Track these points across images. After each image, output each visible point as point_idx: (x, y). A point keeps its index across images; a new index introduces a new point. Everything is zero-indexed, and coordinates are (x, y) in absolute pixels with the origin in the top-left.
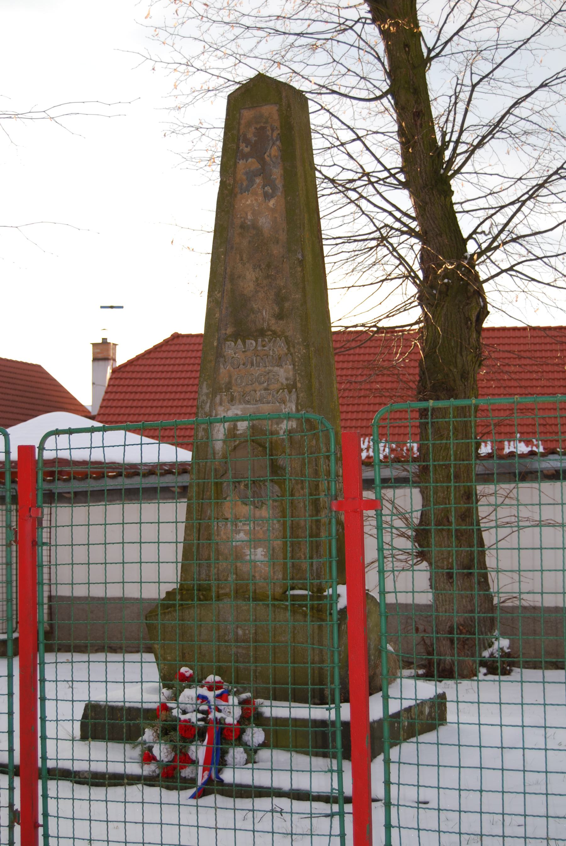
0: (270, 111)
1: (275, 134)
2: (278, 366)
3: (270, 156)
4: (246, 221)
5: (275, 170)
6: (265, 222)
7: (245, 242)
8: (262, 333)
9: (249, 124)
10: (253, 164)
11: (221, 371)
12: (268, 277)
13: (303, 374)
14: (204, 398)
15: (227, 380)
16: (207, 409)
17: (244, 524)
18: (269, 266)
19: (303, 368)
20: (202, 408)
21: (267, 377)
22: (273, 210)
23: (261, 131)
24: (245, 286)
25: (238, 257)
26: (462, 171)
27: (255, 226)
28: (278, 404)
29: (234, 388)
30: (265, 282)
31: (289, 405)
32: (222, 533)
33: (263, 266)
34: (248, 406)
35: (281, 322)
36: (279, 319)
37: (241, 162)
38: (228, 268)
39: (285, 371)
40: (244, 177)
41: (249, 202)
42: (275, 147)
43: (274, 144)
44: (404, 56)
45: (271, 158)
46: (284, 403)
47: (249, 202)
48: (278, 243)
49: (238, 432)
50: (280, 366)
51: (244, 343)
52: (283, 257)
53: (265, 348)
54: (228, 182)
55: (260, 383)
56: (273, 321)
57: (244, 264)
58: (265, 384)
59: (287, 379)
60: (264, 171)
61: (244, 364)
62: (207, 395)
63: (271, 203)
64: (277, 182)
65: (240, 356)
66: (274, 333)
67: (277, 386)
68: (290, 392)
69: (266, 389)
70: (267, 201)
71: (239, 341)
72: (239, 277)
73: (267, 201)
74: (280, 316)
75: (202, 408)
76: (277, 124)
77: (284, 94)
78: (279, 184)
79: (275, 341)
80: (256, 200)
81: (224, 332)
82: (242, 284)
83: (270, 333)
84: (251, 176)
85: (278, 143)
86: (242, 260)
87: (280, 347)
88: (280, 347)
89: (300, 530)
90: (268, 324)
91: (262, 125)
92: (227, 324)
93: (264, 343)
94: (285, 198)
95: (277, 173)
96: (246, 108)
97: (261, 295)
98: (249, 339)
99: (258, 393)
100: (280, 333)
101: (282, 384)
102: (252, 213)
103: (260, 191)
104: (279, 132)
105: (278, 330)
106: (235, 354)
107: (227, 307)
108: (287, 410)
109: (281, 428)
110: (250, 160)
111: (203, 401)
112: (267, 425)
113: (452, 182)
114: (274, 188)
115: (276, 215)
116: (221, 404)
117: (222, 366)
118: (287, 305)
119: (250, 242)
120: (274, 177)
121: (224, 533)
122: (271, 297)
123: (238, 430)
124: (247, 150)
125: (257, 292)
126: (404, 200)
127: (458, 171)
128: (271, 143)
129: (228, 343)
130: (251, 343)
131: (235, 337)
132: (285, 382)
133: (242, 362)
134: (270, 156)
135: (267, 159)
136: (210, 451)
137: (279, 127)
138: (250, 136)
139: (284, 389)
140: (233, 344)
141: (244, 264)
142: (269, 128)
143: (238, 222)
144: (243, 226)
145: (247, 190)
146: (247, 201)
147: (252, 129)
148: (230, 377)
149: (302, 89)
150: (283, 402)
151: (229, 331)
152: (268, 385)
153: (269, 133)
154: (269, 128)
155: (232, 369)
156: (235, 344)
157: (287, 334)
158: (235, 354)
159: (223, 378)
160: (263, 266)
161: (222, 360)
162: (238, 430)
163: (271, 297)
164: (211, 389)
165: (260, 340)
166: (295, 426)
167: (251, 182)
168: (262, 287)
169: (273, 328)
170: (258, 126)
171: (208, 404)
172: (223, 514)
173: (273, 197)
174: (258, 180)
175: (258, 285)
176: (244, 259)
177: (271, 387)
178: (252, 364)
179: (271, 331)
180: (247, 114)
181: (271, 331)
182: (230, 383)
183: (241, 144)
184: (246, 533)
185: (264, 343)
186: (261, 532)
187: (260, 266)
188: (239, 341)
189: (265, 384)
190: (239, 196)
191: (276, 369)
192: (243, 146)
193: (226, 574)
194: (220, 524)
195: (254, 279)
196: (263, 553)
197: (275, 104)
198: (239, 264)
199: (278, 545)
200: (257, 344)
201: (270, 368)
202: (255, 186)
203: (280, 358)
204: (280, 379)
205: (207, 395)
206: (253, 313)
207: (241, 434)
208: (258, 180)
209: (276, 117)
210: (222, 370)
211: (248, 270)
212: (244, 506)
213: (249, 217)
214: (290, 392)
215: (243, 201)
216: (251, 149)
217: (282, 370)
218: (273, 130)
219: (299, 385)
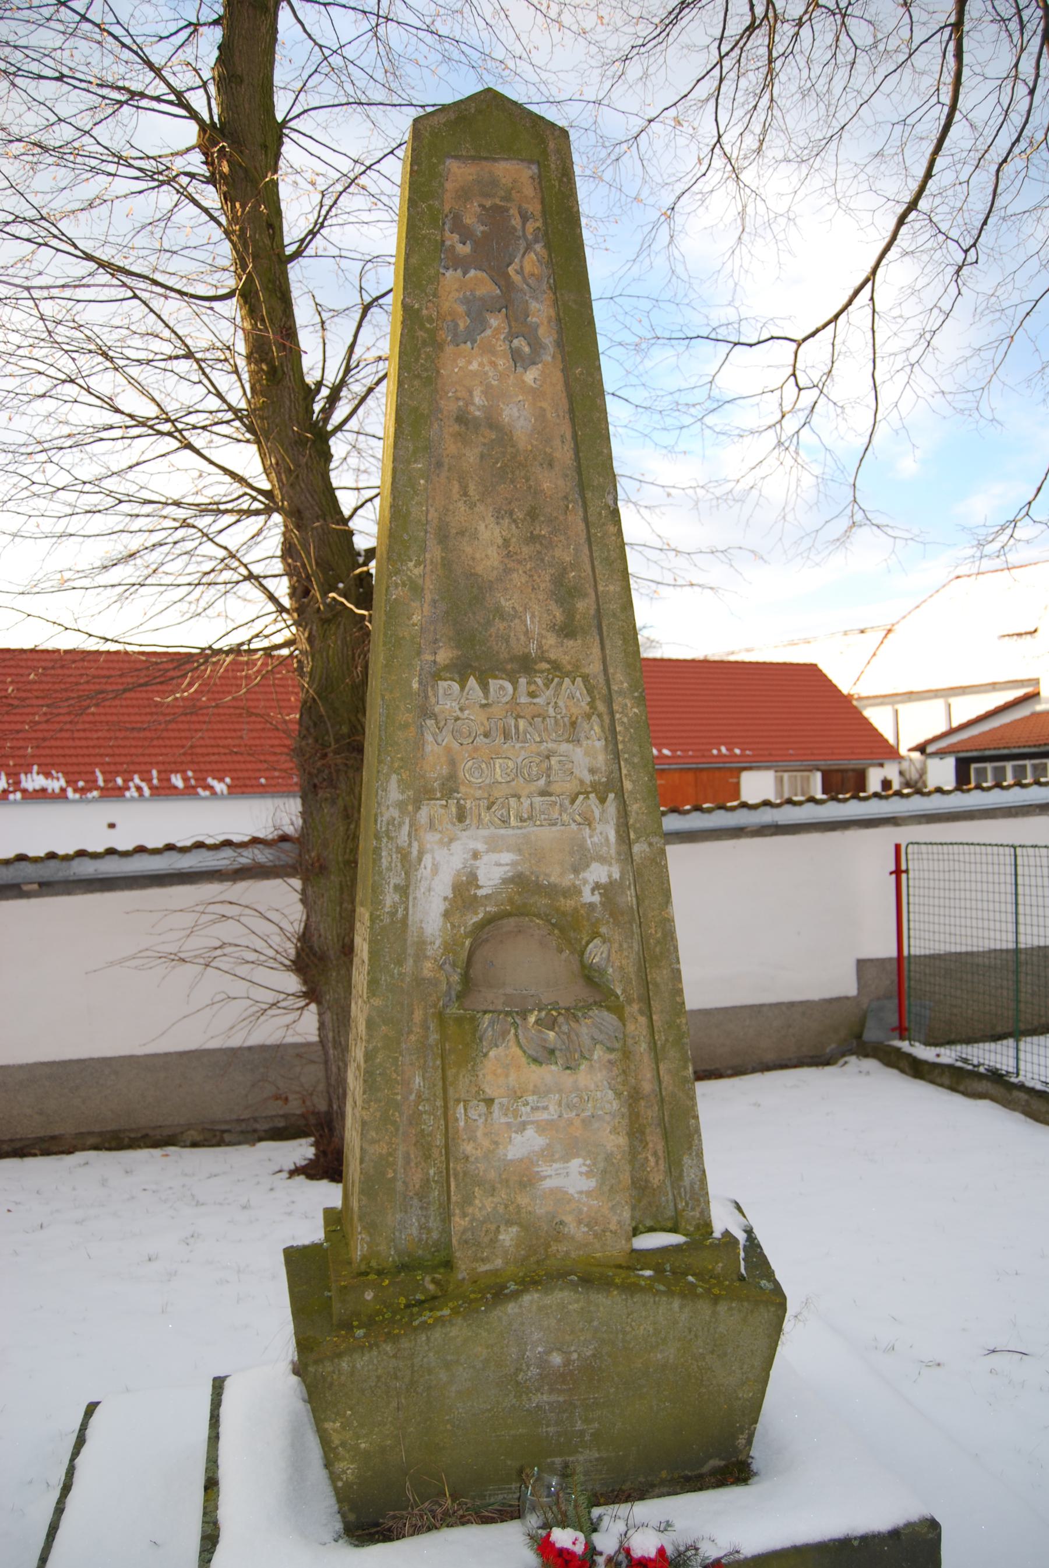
0: (514, 173)
1: (530, 226)
2: (568, 741)
3: (520, 272)
4: (472, 408)
5: (534, 305)
6: (518, 416)
7: (472, 456)
8: (525, 665)
9: (464, 194)
10: (481, 283)
11: (428, 748)
12: (533, 539)
13: (636, 760)
14: (395, 813)
15: (445, 770)
16: (403, 838)
17: (535, 1109)
18: (533, 515)
19: (636, 748)
20: (390, 838)
21: (545, 765)
22: (536, 394)
23: (496, 215)
24: (478, 556)
25: (456, 487)
26: (345, 428)
27: (492, 423)
28: (574, 826)
29: (462, 789)
30: (525, 550)
31: (599, 828)
32: (479, 1134)
33: (519, 515)
34: (503, 831)
35: (571, 643)
36: (566, 636)
37: (449, 274)
38: (432, 510)
39: (587, 753)
40: (461, 309)
41: (474, 366)
42: (532, 255)
43: (528, 248)
44: (267, 242)
45: (524, 277)
46: (589, 825)
47: (474, 366)
48: (551, 465)
49: (481, 892)
50: (574, 740)
51: (485, 687)
52: (566, 498)
53: (535, 701)
54: (425, 312)
55: (529, 781)
56: (551, 640)
57: (472, 506)
58: (542, 782)
59: (592, 771)
60: (507, 301)
61: (486, 735)
62: (401, 805)
63: (530, 376)
64: (541, 331)
65: (475, 718)
66: (556, 666)
67: (571, 786)
68: (603, 800)
69: (543, 793)
70: (520, 370)
71: (472, 682)
72: (462, 533)
73: (520, 370)
74: (567, 630)
75: (390, 838)
76: (534, 207)
77: (552, 145)
78: (547, 337)
79: (560, 684)
80: (493, 364)
81: (428, 657)
82: (469, 550)
83: (545, 666)
84: (478, 310)
85: (538, 247)
86: (465, 494)
87: (572, 697)
88: (572, 697)
89: (643, 1103)
90: (540, 646)
91: (497, 201)
92: (435, 641)
93: (533, 688)
94: (564, 370)
95: (540, 311)
96: (456, 157)
97: (518, 578)
98: (496, 677)
99: (526, 803)
100: (569, 667)
101: (582, 782)
102: (485, 393)
103: (501, 346)
104: (539, 224)
105: (565, 660)
106: (461, 709)
107: (434, 602)
108: (595, 839)
109: (585, 882)
110: (472, 273)
111: (391, 822)
112: (556, 875)
113: (332, 442)
114: (536, 345)
115: (544, 405)
116: (432, 826)
117: (429, 738)
118: (581, 605)
119: (482, 456)
120: (532, 319)
121: (485, 1134)
122: (543, 586)
123: (479, 887)
124: (464, 250)
125: (507, 571)
126: (247, 459)
127: (339, 428)
128: (522, 245)
129: (443, 685)
130: (502, 688)
131: (461, 670)
132: (588, 778)
133: (481, 731)
134: (520, 272)
135: (516, 278)
136: (412, 936)
137: (538, 213)
138: (469, 220)
139: (587, 793)
140: (456, 686)
141: (472, 506)
142: (514, 211)
143: (449, 407)
144: (462, 419)
145: (470, 336)
146: (470, 363)
147: (474, 207)
148: (453, 763)
149: (218, 234)
150: (588, 821)
151: (444, 656)
152: (549, 783)
153: (516, 222)
154: (514, 211)
155: (455, 745)
156: (463, 688)
157: (586, 671)
158: (461, 709)
159: (434, 768)
160: (519, 515)
161: (430, 722)
162: (479, 887)
163: (543, 586)
164: (411, 793)
165: (523, 681)
166: (616, 876)
167: (479, 323)
168: (519, 562)
169: (553, 656)
170: (488, 203)
171: (406, 829)
172: (480, 1090)
173: (534, 363)
174: (495, 321)
175: (509, 555)
176: (471, 493)
177: (555, 788)
178: (507, 736)
179: (549, 662)
180: (458, 172)
181: (549, 662)
182: (452, 777)
183: (447, 234)
184: (542, 1128)
185: (533, 688)
186: (577, 1122)
187: (511, 513)
188: (472, 682)
189: (542, 782)
190: (449, 349)
191: (564, 747)
192: (452, 239)
193: (493, 1227)
194: (473, 1114)
195: (500, 541)
196: (584, 1169)
197: (531, 162)
198: (460, 504)
199: (618, 1147)
200: (515, 689)
201: (550, 745)
202: (489, 332)
203: (573, 724)
204: (577, 772)
205: (401, 805)
206: (502, 618)
207: (487, 897)
208: (495, 321)
209: (529, 191)
210: (430, 747)
211: (483, 519)
212: (533, 1067)
213: (477, 400)
214: (603, 800)
215: (461, 362)
216: (474, 250)
217: (578, 750)
218: (525, 218)
219: (628, 785)
